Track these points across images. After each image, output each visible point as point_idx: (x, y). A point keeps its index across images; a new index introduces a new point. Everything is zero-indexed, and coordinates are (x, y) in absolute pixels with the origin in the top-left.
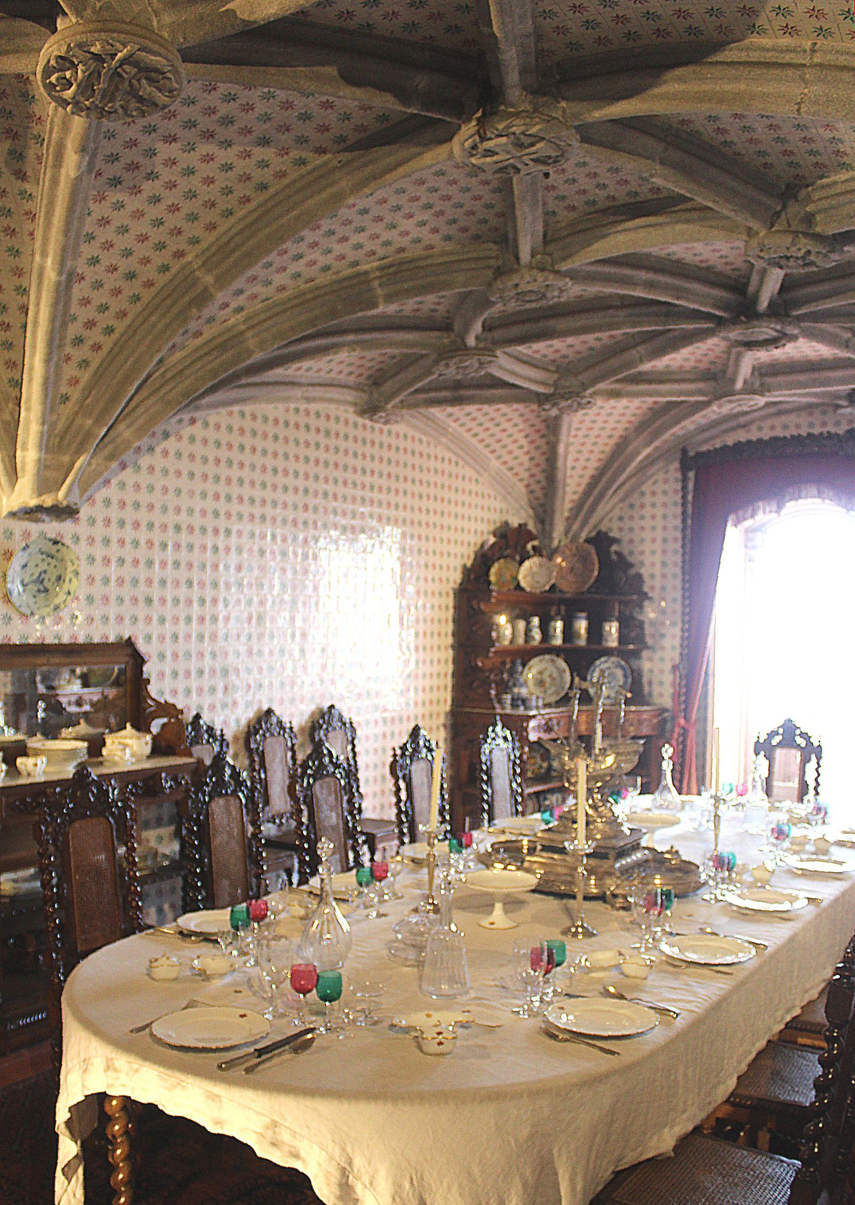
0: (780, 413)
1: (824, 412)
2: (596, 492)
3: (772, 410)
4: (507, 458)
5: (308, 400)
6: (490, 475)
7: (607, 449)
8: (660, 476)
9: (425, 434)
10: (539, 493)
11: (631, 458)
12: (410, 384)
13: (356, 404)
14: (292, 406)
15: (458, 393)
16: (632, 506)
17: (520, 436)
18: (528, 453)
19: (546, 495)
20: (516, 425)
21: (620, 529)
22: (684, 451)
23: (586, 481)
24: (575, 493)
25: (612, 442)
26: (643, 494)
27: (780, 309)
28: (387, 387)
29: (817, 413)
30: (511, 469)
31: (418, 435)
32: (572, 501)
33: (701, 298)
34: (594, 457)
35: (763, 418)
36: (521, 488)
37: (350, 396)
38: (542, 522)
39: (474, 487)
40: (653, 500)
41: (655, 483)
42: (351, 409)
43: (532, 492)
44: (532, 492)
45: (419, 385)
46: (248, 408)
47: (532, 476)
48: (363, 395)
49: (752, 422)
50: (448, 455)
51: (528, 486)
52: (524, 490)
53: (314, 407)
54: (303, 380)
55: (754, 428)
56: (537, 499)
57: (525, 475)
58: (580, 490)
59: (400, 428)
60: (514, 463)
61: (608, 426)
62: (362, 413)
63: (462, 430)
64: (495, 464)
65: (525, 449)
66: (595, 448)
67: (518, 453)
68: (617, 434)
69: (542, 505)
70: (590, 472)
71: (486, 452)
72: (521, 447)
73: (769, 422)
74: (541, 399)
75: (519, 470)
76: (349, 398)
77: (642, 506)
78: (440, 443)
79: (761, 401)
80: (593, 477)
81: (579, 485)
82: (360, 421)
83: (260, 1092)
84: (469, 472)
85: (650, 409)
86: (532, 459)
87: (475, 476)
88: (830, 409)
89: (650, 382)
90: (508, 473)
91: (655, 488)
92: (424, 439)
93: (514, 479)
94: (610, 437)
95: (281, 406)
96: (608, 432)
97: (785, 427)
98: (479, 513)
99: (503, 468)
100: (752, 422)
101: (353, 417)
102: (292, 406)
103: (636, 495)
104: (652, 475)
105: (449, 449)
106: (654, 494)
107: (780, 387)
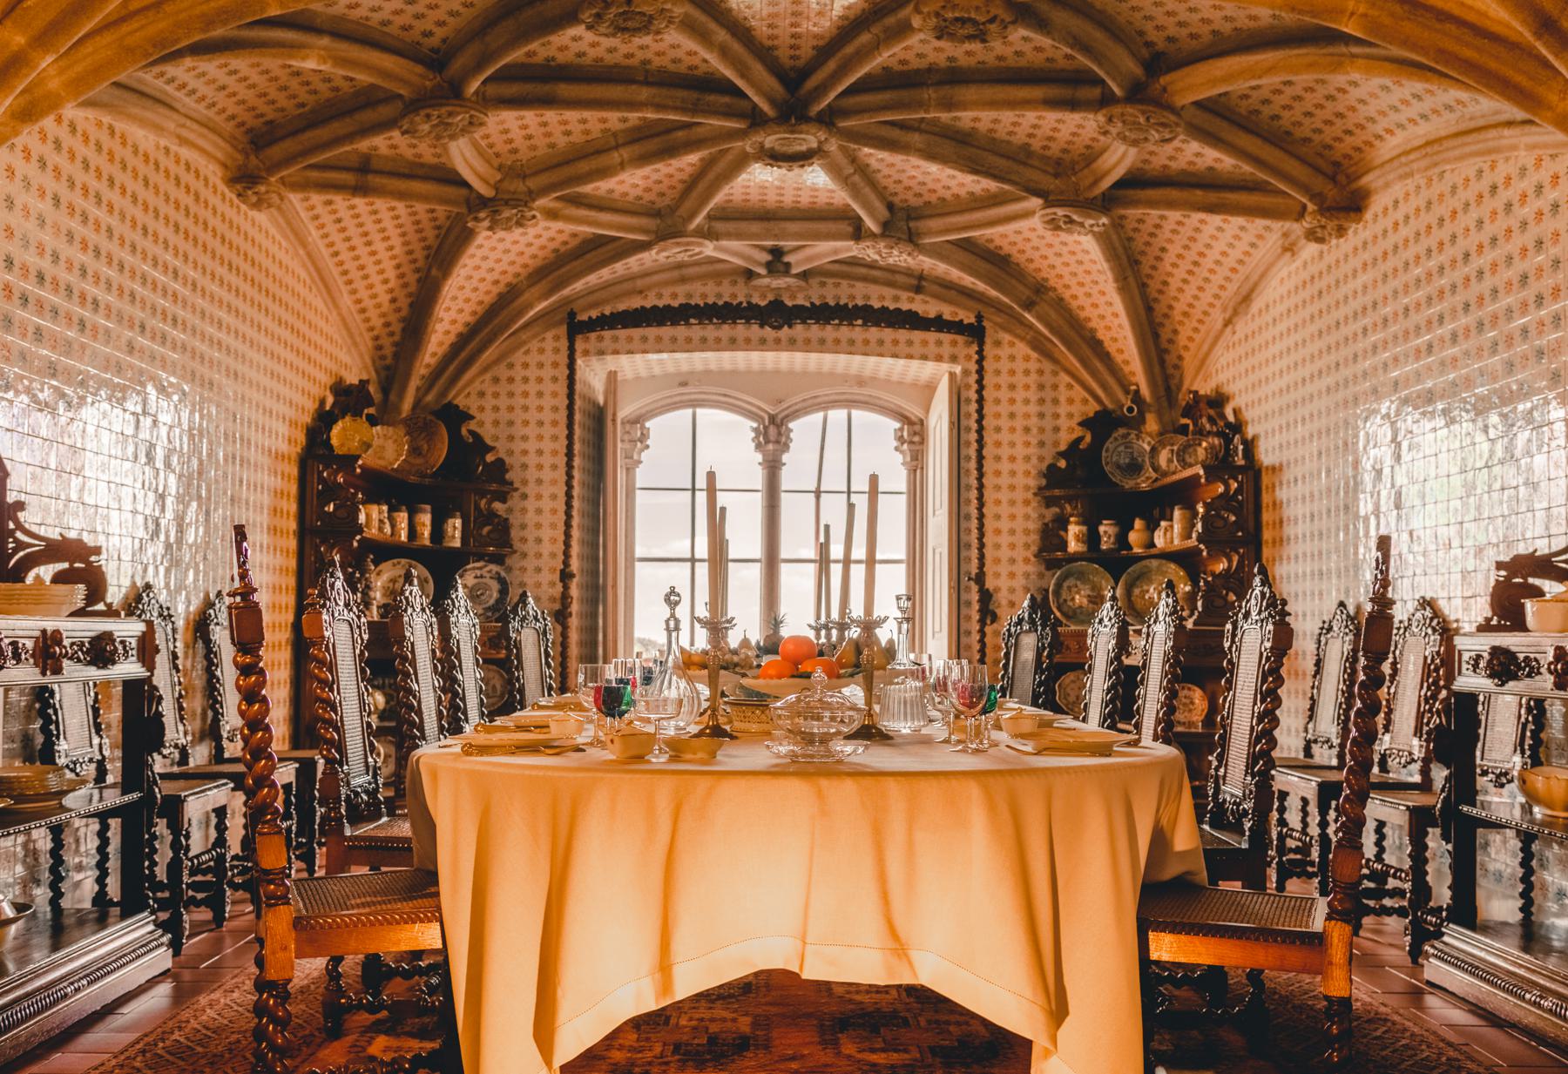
0: (683, 280)
1: (735, 283)
2: (463, 355)
3: (676, 274)
4: (363, 294)
5: (183, 141)
6: (340, 314)
7: (488, 300)
8: (534, 345)
9: (286, 237)
10: (388, 351)
11: (521, 313)
12: (305, 153)
13: (225, 166)
14: (163, 142)
15: (364, 178)
16: (496, 380)
17: (388, 265)
18: (391, 291)
19: (396, 355)
20: (391, 248)
21: (482, 409)
22: (572, 315)
23: (452, 338)
24: (434, 354)
25: (496, 290)
26: (511, 366)
27: (827, 120)
28: (277, 151)
29: (726, 282)
30: (363, 311)
31: (278, 237)
32: (428, 366)
33: (759, 90)
34: (468, 308)
35: (667, 283)
36: (366, 343)
37: (221, 149)
38: (385, 390)
39: (322, 324)
40: (524, 373)
41: (527, 352)
42: (220, 172)
43: (379, 348)
44: (379, 348)
45: (313, 161)
46: (120, 126)
47: (387, 325)
48: (240, 157)
49: (649, 288)
50: (303, 275)
51: (376, 338)
52: (370, 344)
53: (185, 153)
54: (178, 106)
55: (652, 294)
56: (383, 358)
57: (377, 322)
58: (441, 351)
59: (261, 217)
60: (368, 303)
61: (499, 268)
62: (232, 181)
63: (321, 244)
64: (346, 301)
65: (390, 285)
66: (473, 296)
67: (380, 289)
68: (509, 278)
69: (387, 368)
70: (459, 328)
71: (340, 280)
72: (386, 281)
73: (667, 292)
74: (476, 204)
75: (373, 314)
76: (219, 155)
77: (511, 380)
78: (297, 254)
79: (709, 249)
80: (460, 335)
81: (441, 344)
82: (226, 191)
83: (560, 992)
84: (321, 306)
85: (556, 251)
86: (393, 300)
87: (325, 311)
88: (741, 281)
89: (591, 207)
90: (359, 318)
91: (528, 359)
92: (284, 244)
93: (363, 326)
94: (496, 282)
95: (152, 137)
96: (496, 275)
97: (690, 296)
98: (326, 362)
99: (354, 308)
100: (649, 288)
101: (222, 187)
102: (163, 142)
103: (502, 366)
104: (525, 343)
105: (304, 265)
106: (526, 366)
107: (729, 236)
